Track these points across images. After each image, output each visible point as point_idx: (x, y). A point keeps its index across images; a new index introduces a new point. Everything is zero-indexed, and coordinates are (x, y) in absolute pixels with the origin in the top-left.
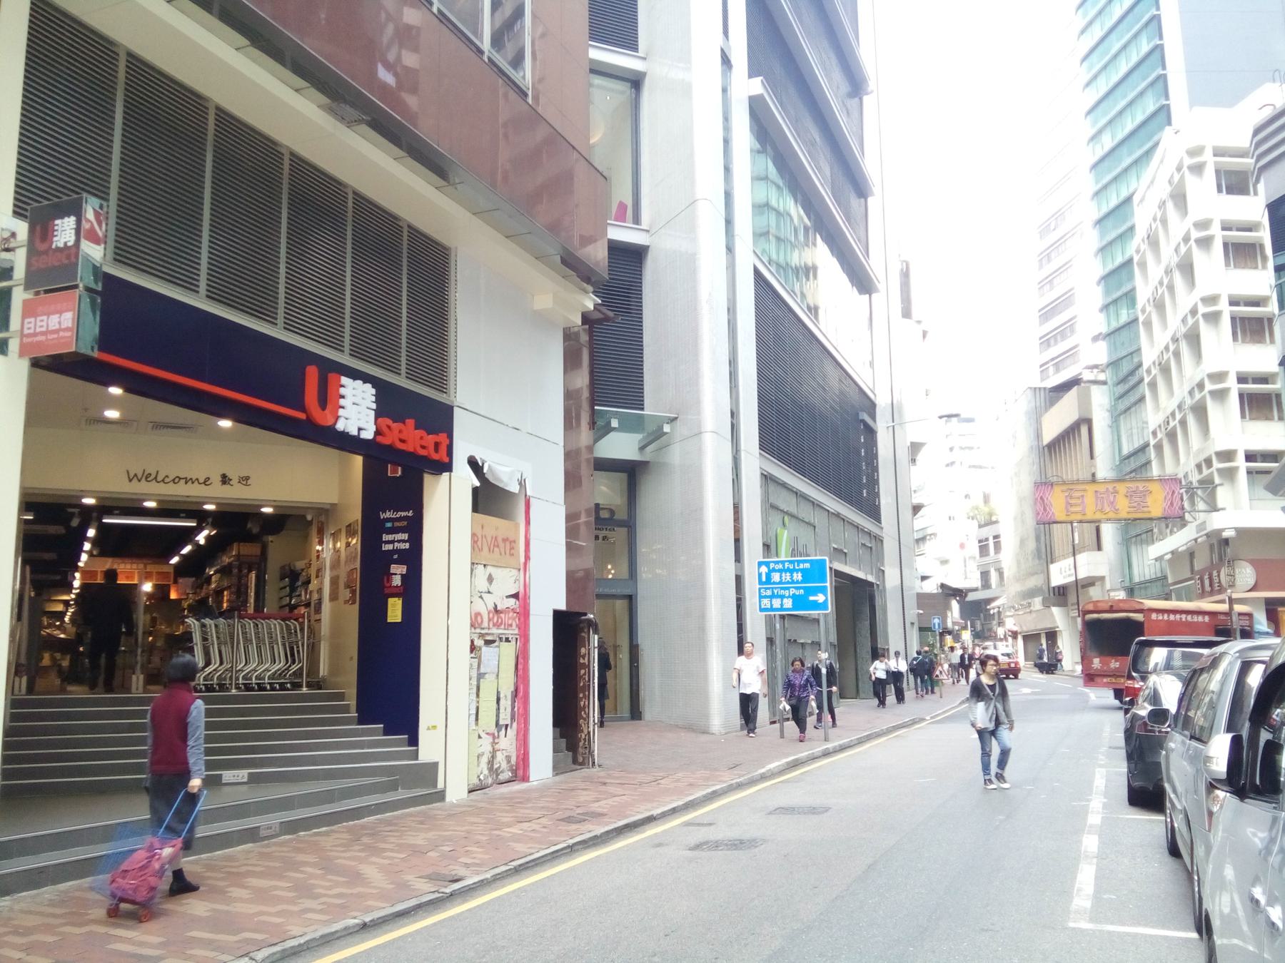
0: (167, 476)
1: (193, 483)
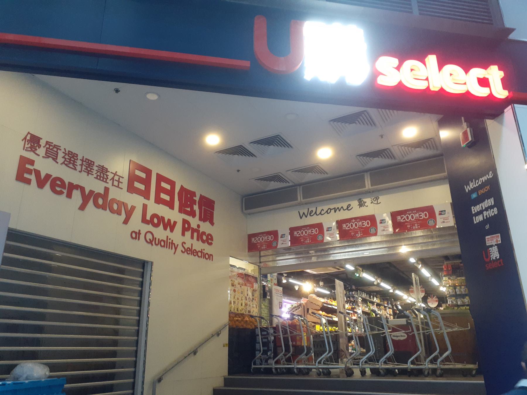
0: (323, 210)
1: (339, 211)
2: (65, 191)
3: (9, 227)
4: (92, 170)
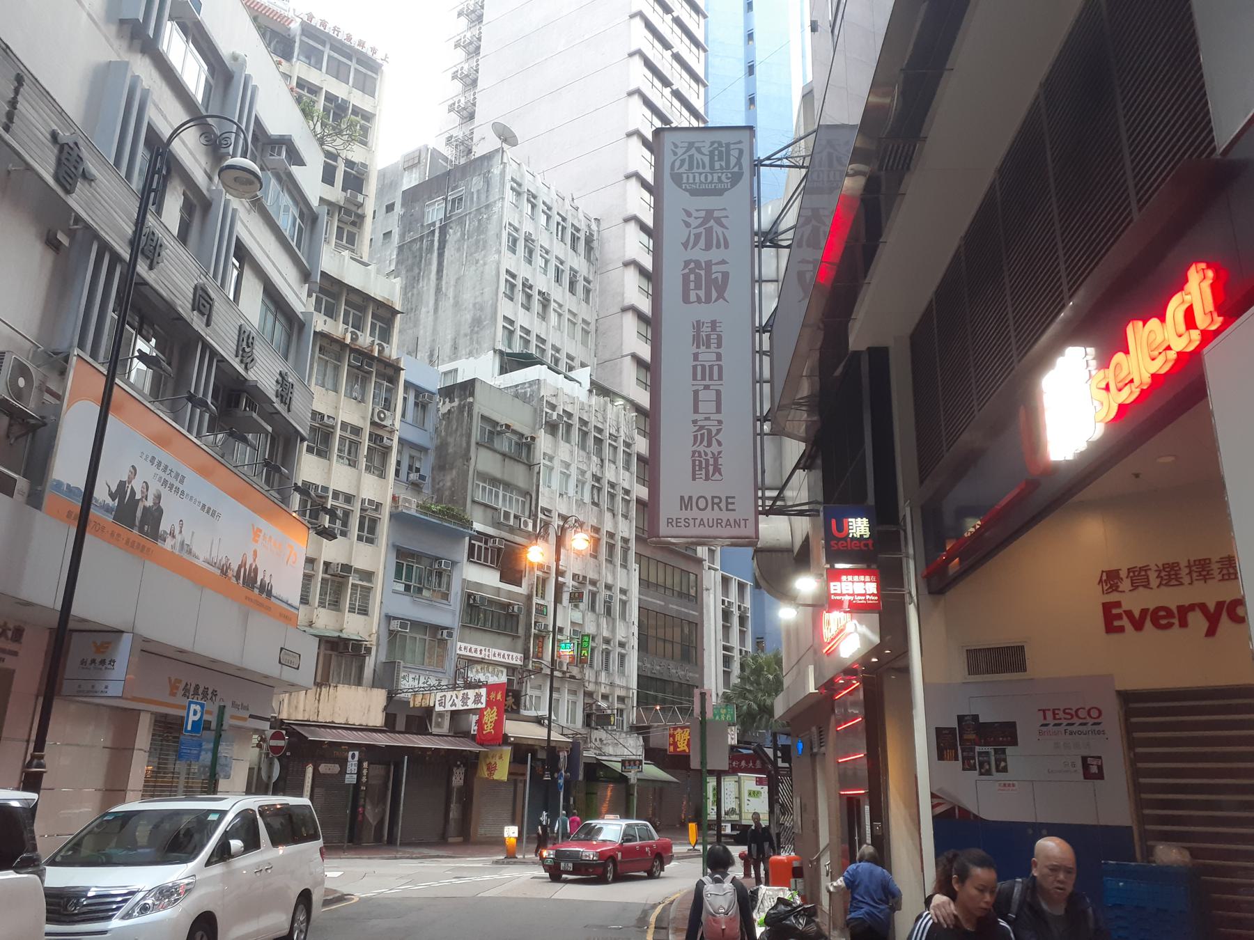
2: (1176, 621)
3: (1117, 689)
4: (1211, 572)
